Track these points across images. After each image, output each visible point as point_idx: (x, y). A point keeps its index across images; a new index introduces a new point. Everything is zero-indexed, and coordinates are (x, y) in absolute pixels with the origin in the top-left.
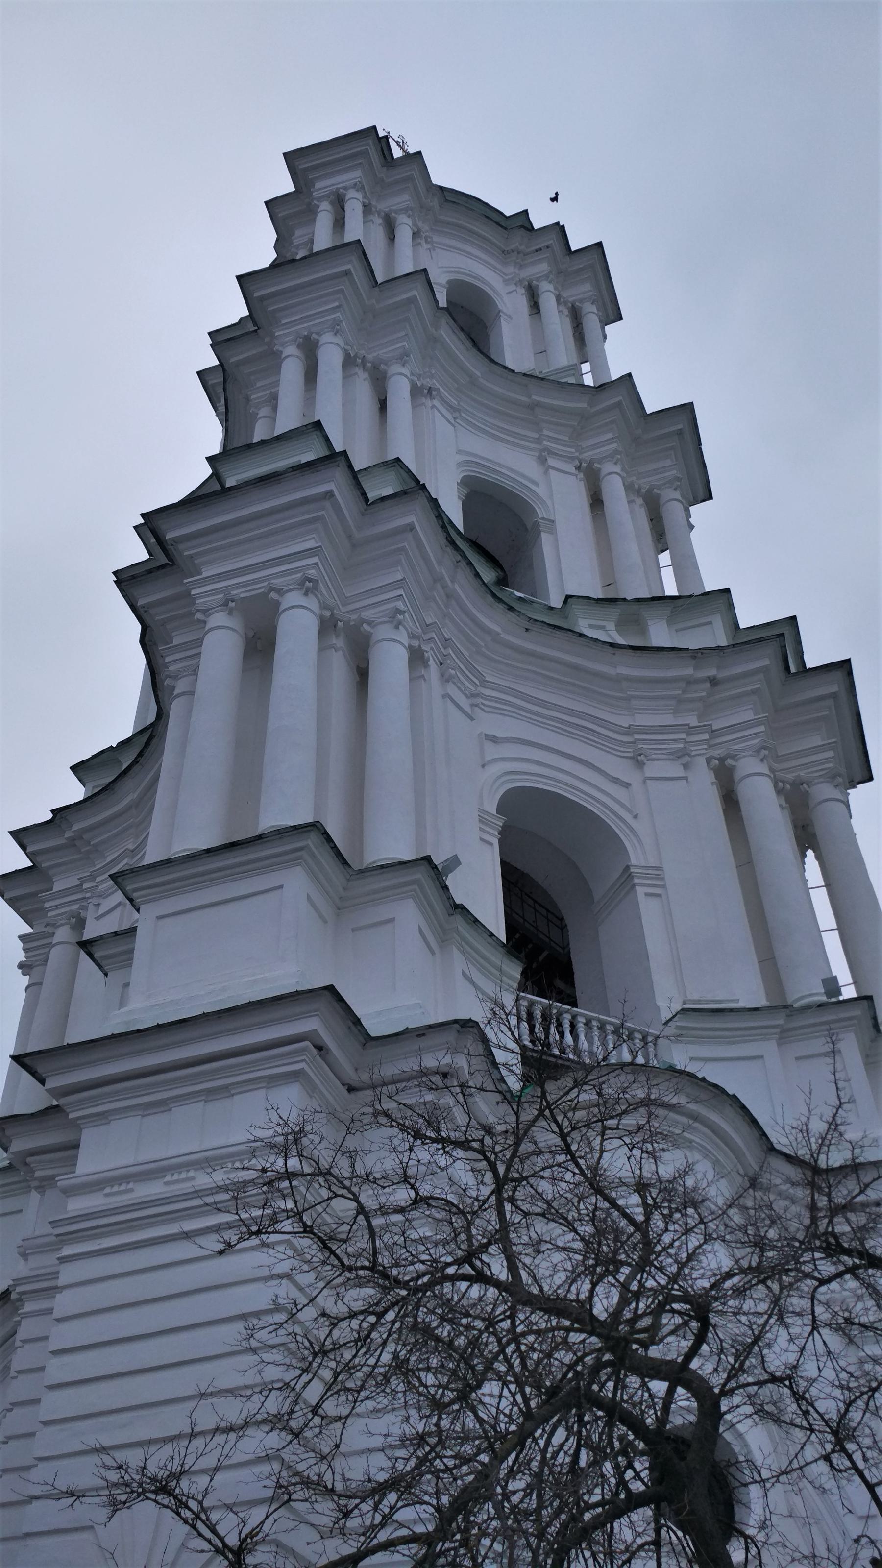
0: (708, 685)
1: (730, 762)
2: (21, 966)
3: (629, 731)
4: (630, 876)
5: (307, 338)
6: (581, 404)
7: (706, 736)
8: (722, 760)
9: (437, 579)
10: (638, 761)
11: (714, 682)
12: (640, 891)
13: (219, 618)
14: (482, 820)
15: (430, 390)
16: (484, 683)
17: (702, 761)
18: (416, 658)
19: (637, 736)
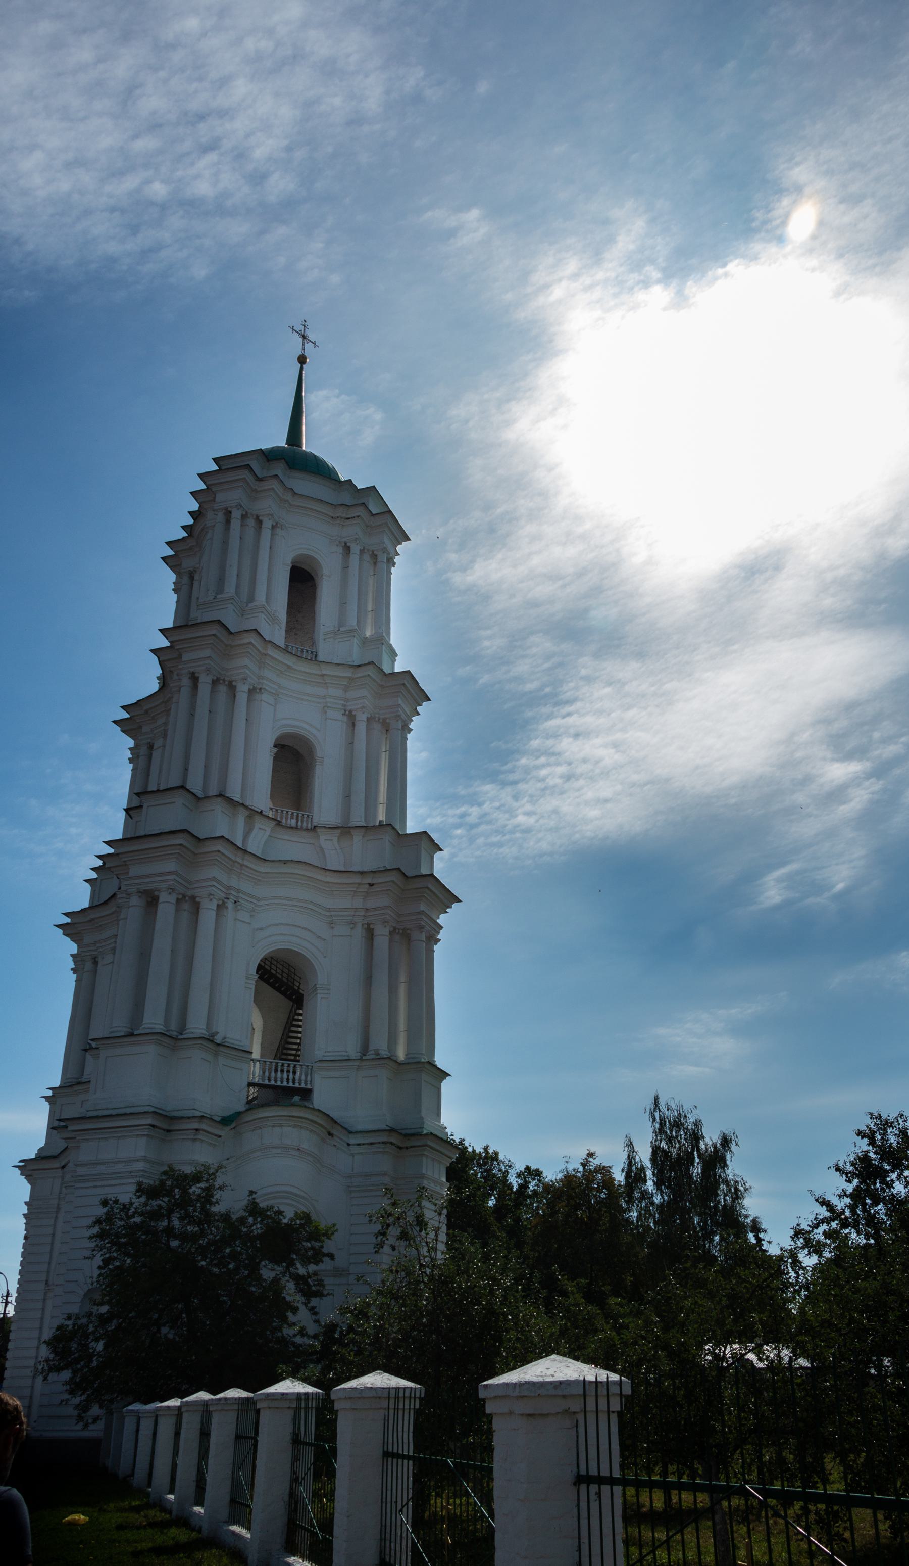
0: (367, 886)
1: (372, 926)
2: (72, 969)
3: (329, 910)
4: (316, 989)
5: (193, 674)
6: (348, 673)
7: (363, 913)
8: (368, 924)
9: (235, 862)
10: (331, 924)
11: (371, 885)
12: (319, 996)
13: (135, 900)
14: (247, 978)
15: (260, 689)
16: (258, 899)
17: (360, 925)
18: (221, 907)
19: (333, 913)
